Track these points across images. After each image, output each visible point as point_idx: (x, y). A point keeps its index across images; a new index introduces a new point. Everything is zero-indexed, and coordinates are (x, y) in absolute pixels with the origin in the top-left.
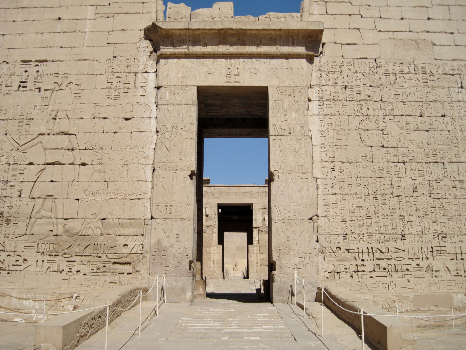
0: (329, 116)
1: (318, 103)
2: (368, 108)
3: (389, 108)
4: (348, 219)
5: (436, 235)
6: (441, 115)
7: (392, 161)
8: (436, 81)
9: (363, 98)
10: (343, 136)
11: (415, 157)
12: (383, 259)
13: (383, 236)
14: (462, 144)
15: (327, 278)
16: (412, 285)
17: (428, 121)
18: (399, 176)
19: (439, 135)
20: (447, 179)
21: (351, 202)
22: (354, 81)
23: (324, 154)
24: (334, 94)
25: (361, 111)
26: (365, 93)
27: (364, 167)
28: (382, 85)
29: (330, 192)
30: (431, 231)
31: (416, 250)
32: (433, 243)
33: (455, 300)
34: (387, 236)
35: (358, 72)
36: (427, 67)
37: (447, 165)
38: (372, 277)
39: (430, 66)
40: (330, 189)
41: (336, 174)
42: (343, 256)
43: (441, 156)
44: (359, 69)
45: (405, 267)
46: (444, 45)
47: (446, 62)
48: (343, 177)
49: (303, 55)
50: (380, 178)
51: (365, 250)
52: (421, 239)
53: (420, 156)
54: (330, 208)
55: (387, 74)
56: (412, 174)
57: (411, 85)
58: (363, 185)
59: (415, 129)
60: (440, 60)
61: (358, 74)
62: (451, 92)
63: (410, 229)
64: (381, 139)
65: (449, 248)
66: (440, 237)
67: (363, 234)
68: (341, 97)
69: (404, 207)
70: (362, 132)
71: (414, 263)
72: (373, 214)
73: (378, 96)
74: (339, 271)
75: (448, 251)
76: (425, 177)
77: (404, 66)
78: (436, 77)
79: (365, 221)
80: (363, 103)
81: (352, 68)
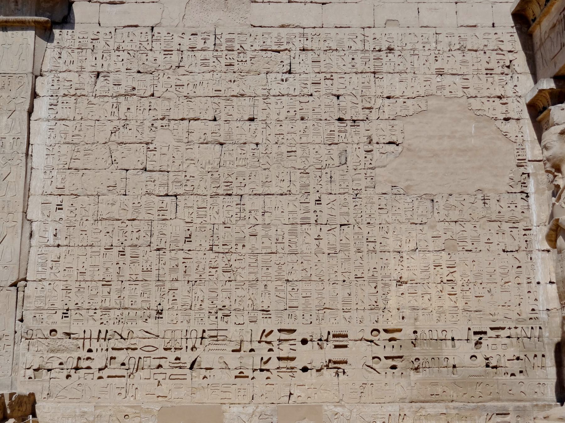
0: (63, 122)
1: (50, 101)
2: (129, 109)
3: (161, 107)
4: (74, 286)
5: (213, 311)
6: (247, 118)
7: (157, 192)
8: (248, 62)
9: (123, 92)
10: (83, 153)
11: (196, 187)
12: (123, 349)
13: (126, 312)
14: (275, 165)
15: (30, 378)
16: (164, 390)
17: (225, 128)
18: (164, 217)
19: (240, 151)
20: (244, 222)
21: (83, 259)
22: (112, 63)
23: (49, 182)
24: (78, 86)
25: (116, 114)
26: (127, 82)
27: (111, 202)
28: (158, 70)
29: (51, 242)
30: (206, 305)
31: (178, 335)
32: (207, 324)
33: (227, 415)
34: (132, 313)
35: (121, 49)
36: (236, 39)
37: (246, 199)
38: (100, 378)
39: (243, 38)
40: (52, 237)
41: (62, 214)
42: (58, 344)
43: (239, 185)
44: (123, 45)
45: (157, 362)
46: (269, 2)
47: (269, 30)
48: (74, 219)
49: (29, 22)
50: (134, 220)
51: (95, 335)
52: (187, 318)
53: (202, 184)
54: (48, 268)
55: (168, 52)
56: (187, 215)
57: (206, 69)
58: (104, 232)
59: (202, 141)
60: (261, 27)
61: (121, 53)
62: (269, 81)
63: (171, 302)
64: (143, 158)
65: (233, 332)
66: (220, 314)
67: (95, 309)
68: (88, 89)
69: (167, 267)
70: (114, 147)
71: (171, 356)
72: (115, 278)
73: (149, 87)
74: (50, 368)
75: (229, 336)
76: (207, 219)
77: (199, 38)
78: (249, 54)
79: (101, 288)
80: (121, 99)
81: (111, 43)
